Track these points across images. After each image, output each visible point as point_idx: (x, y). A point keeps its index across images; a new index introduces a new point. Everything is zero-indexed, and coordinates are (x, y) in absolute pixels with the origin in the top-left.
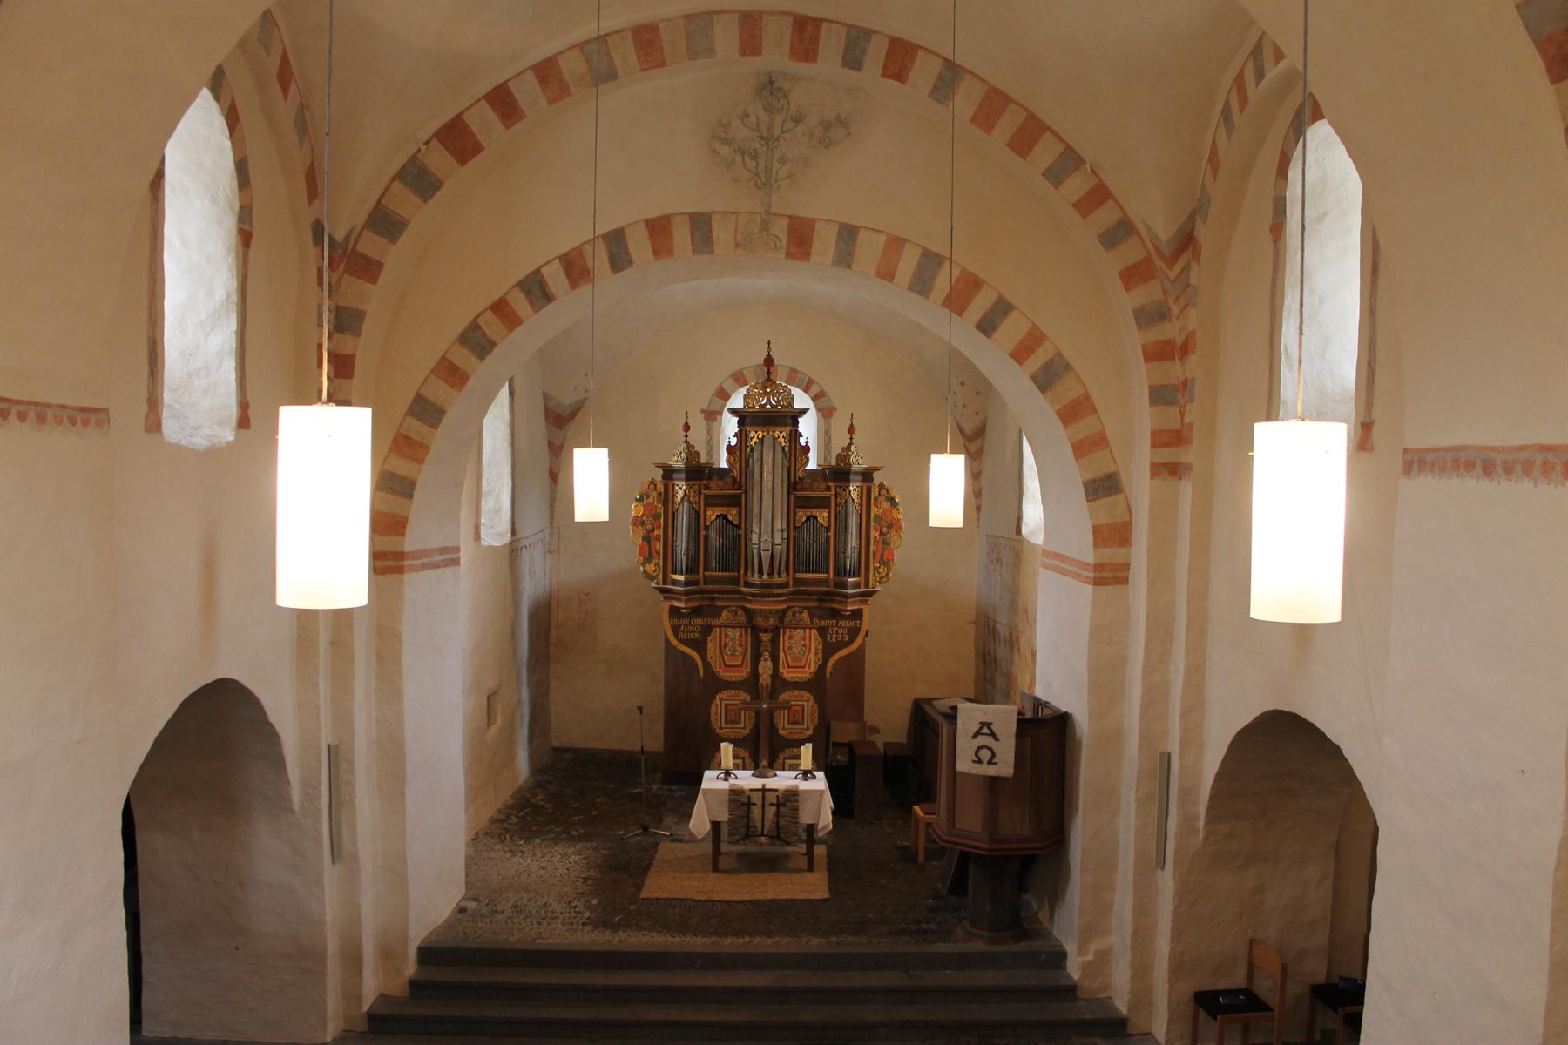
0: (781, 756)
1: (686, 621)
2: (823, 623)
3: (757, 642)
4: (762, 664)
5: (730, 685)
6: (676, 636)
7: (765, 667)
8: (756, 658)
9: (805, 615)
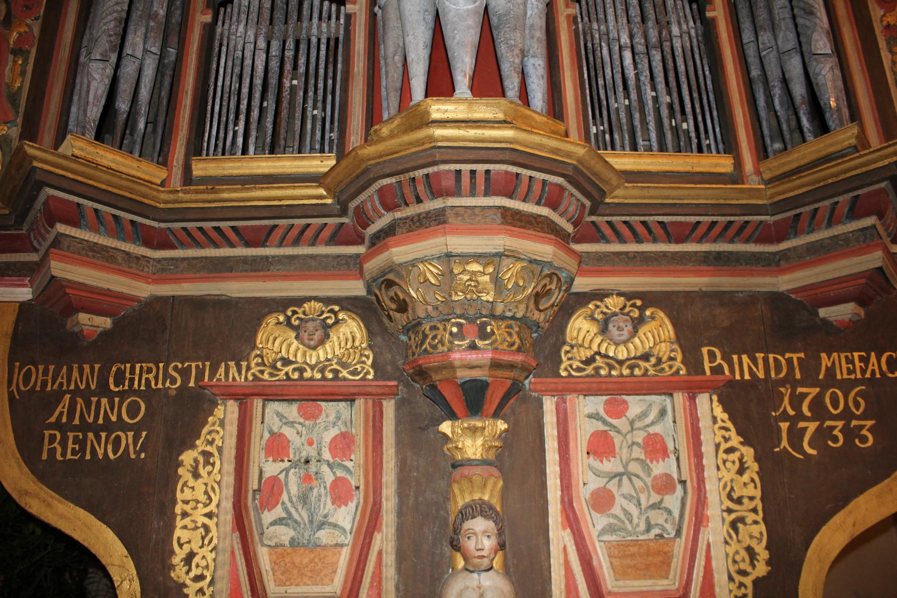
1: (86, 375)
2: (745, 367)
3: (427, 469)
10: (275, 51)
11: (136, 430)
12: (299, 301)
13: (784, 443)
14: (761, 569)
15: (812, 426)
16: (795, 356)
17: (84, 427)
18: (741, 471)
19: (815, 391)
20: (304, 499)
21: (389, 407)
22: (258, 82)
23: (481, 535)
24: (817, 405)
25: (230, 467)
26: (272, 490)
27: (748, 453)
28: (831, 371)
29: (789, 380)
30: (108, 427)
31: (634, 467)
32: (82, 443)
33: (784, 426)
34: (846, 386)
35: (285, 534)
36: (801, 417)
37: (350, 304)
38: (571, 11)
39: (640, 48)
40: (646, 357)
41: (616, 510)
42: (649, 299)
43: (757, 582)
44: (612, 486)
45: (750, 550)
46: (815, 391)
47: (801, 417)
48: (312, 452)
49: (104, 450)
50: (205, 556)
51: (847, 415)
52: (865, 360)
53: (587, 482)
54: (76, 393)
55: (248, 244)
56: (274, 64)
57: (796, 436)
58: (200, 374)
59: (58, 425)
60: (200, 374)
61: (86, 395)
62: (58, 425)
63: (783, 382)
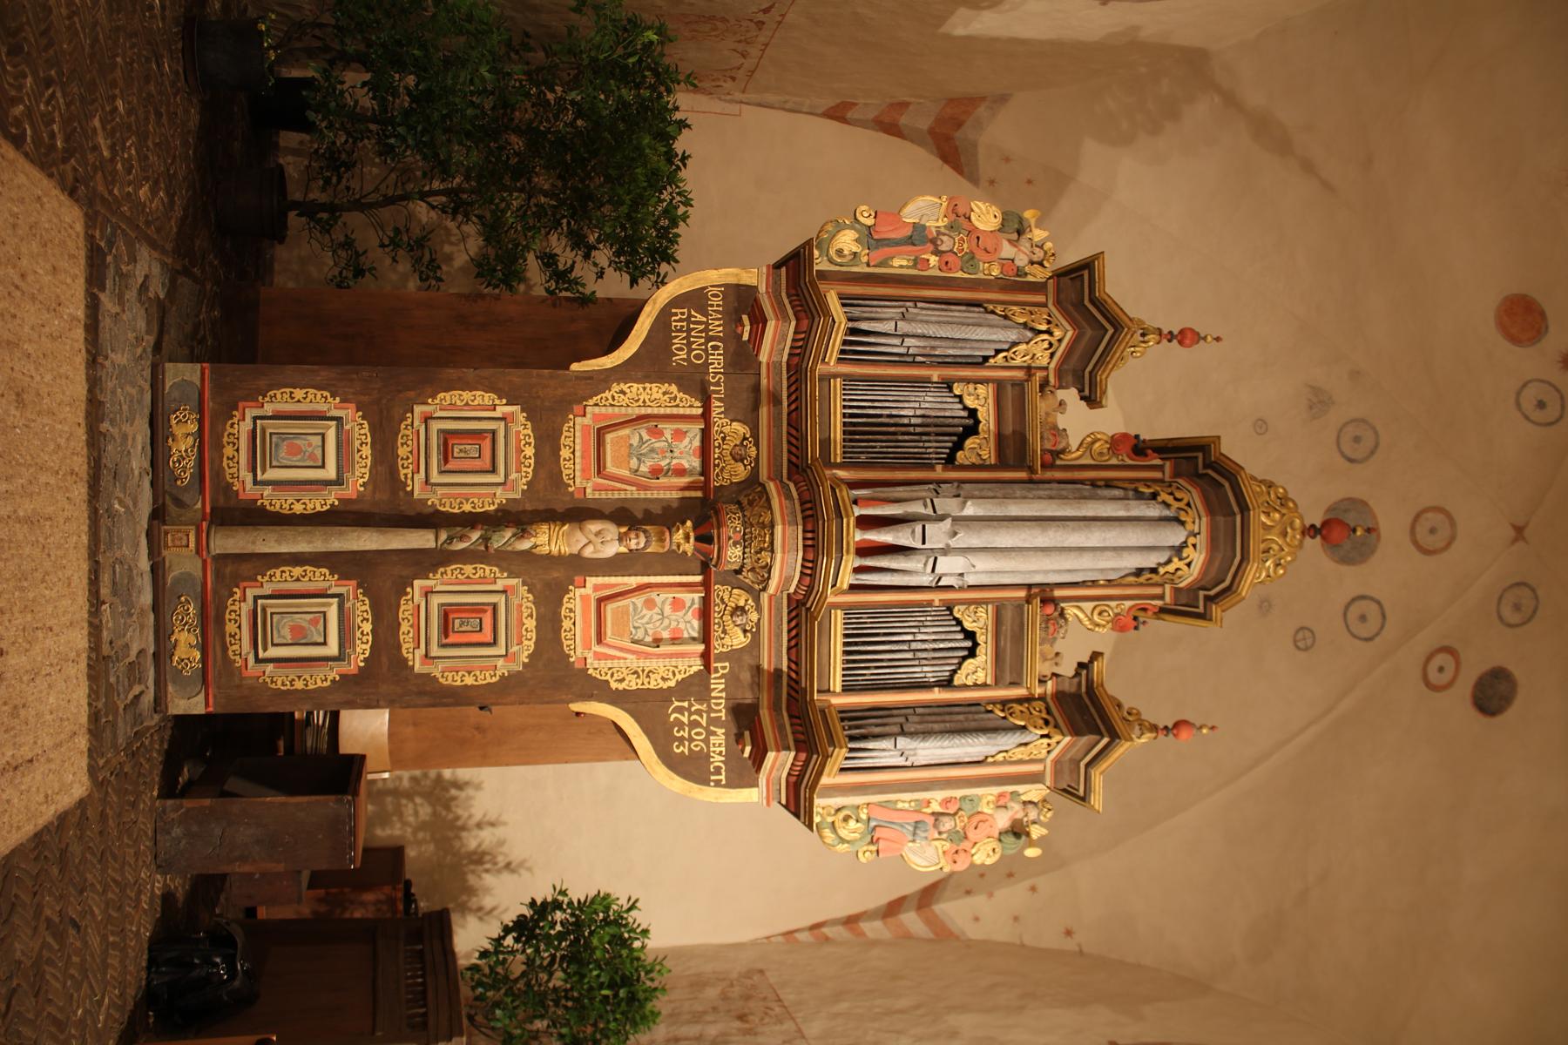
0: (348, 588)
1: (717, 328)
4: (611, 530)
5: (548, 443)
6: (678, 301)
7: (604, 541)
8: (625, 516)
9: (738, 640)
10: (914, 421)
11: (688, 360)
12: (757, 445)
13: (677, 704)
14: (614, 685)
15: (685, 720)
16: (723, 714)
17: (689, 331)
18: (663, 679)
20: (652, 450)
21: (699, 494)
22: (894, 412)
23: (637, 542)
24: (694, 724)
25: (668, 411)
26: (656, 433)
27: (672, 684)
28: (714, 733)
29: (710, 710)
30: (689, 344)
31: (666, 622)
33: (686, 704)
34: (707, 741)
35: (635, 441)
36: (691, 714)
37: (755, 471)
38: (937, 603)
39: (914, 646)
40: (724, 632)
42: (756, 636)
44: (657, 610)
45: (623, 680)
47: (691, 714)
50: (624, 400)
51: (691, 740)
52: (720, 753)
54: (707, 324)
56: (906, 421)
57: (680, 710)
58: (718, 392)
59: (690, 315)
60: (718, 392)
61: (706, 330)
62: (690, 315)
63: (709, 706)
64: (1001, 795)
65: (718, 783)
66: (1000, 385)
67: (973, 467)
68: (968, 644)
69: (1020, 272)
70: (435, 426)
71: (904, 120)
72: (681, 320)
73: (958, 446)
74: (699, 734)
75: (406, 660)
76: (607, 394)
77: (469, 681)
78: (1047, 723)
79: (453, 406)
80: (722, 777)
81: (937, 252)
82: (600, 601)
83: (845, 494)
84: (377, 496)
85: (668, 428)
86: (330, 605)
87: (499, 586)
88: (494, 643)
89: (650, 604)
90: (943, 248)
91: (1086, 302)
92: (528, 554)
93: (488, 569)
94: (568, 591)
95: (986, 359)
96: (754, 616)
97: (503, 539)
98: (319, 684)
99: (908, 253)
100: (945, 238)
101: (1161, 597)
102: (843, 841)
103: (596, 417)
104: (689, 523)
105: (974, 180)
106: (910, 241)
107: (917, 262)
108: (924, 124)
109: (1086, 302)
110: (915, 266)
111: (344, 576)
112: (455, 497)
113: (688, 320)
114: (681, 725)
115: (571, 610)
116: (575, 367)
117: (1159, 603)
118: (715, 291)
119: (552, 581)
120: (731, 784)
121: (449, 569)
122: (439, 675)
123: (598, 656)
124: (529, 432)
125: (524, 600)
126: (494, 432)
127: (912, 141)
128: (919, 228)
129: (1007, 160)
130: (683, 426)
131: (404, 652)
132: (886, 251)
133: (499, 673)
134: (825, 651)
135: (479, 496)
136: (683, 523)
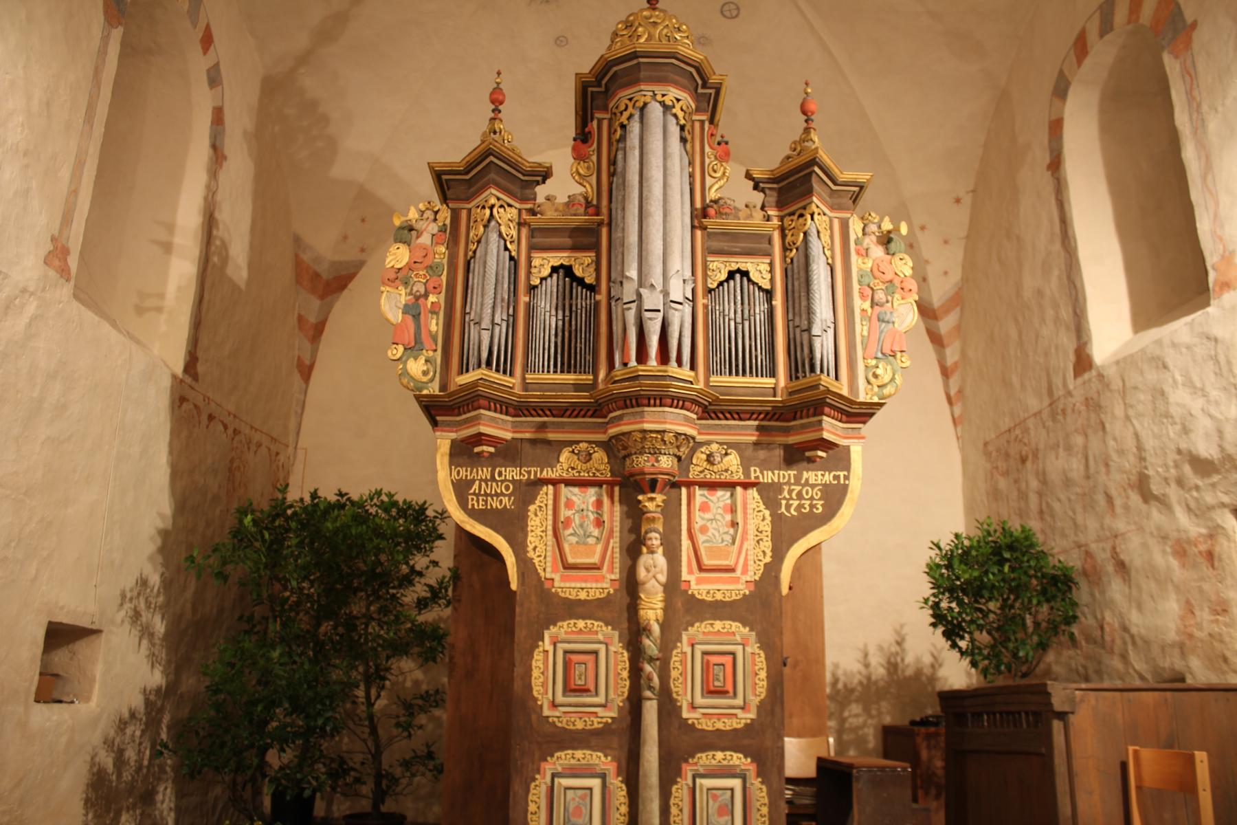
0: (688, 770)
1: (485, 473)
4: (645, 559)
5: (575, 609)
7: (653, 566)
8: (634, 549)
9: (733, 460)
10: (560, 317)
11: (509, 496)
12: (578, 442)
13: (783, 509)
14: (768, 559)
15: (796, 503)
16: (792, 473)
17: (486, 495)
19: (799, 488)
20: (581, 526)
21: (617, 489)
22: (553, 332)
23: (655, 539)
25: (550, 512)
27: (767, 513)
28: (807, 480)
29: (788, 483)
30: (497, 495)
31: (718, 517)
32: (486, 502)
34: (813, 486)
35: (574, 539)
36: (791, 499)
37: (599, 444)
38: (705, 301)
39: (739, 320)
40: (726, 471)
41: (709, 534)
43: (765, 565)
44: (708, 524)
45: (764, 552)
46: (799, 488)
47: (791, 499)
48: (584, 506)
49: (495, 504)
50: (541, 548)
51: (812, 498)
53: (698, 525)
54: (481, 480)
55: (554, 416)
56: (560, 323)
57: (788, 507)
59: (474, 494)
61: (486, 481)
62: (474, 494)
64: (858, 253)
65: (846, 478)
66: (532, 248)
67: (598, 270)
68: (738, 276)
69: (443, 230)
70: (560, 698)
71: (312, 319)
72: (478, 501)
73: (581, 281)
74: (808, 492)
75: (746, 725)
76: (536, 561)
77: (763, 674)
78: (801, 216)
79: (544, 684)
80: (842, 474)
81: (426, 296)
82: (701, 569)
83: (619, 372)
84: (615, 745)
85: (564, 513)
86: (701, 785)
87: (688, 650)
88: (733, 654)
89: (704, 530)
90: (422, 290)
91: (467, 177)
92: (663, 626)
93: (674, 658)
94: (693, 595)
95: (511, 258)
96: (714, 447)
97: (651, 646)
98: (764, 794)
99: (426, 318)
100: (415, 289)
101: (702, 122)
102: (893, 379)
103: (554, 570)
104: (640, 498)
105: (361, 264)
106: (416, 317)
107: (434, 312)
108: (316, 303)
109: (467, 177)
110: (437, 313)
111: (679, 773)
112: (616, 683)
113: (478, 495)
114: (800, 506)
115: (708, 593)
116: (514, 586)
117: (707, 125)
118: (454, 473)
119: (684, 608)
120: (847, 466)
121: (674, 690)
122: (758, 699)
123: (745, 571)
124: (565, 624)
125: (699, 629)
126: (566, 652)
127: (328, 313)
128: (406, 310)
129: (345, 238)
130: (563, 500)
131: (739, 726)
132: (424, 335)
133: (757, 651)
134: (749, 391)
135: (616, 664)
136: (640, 502)
